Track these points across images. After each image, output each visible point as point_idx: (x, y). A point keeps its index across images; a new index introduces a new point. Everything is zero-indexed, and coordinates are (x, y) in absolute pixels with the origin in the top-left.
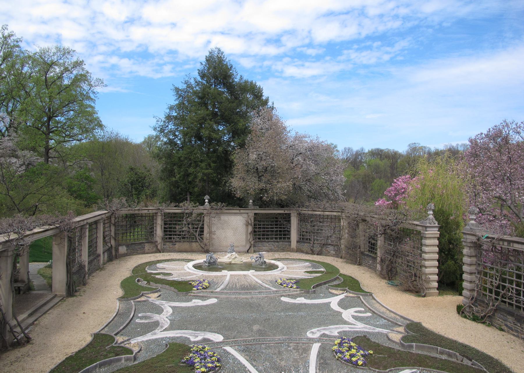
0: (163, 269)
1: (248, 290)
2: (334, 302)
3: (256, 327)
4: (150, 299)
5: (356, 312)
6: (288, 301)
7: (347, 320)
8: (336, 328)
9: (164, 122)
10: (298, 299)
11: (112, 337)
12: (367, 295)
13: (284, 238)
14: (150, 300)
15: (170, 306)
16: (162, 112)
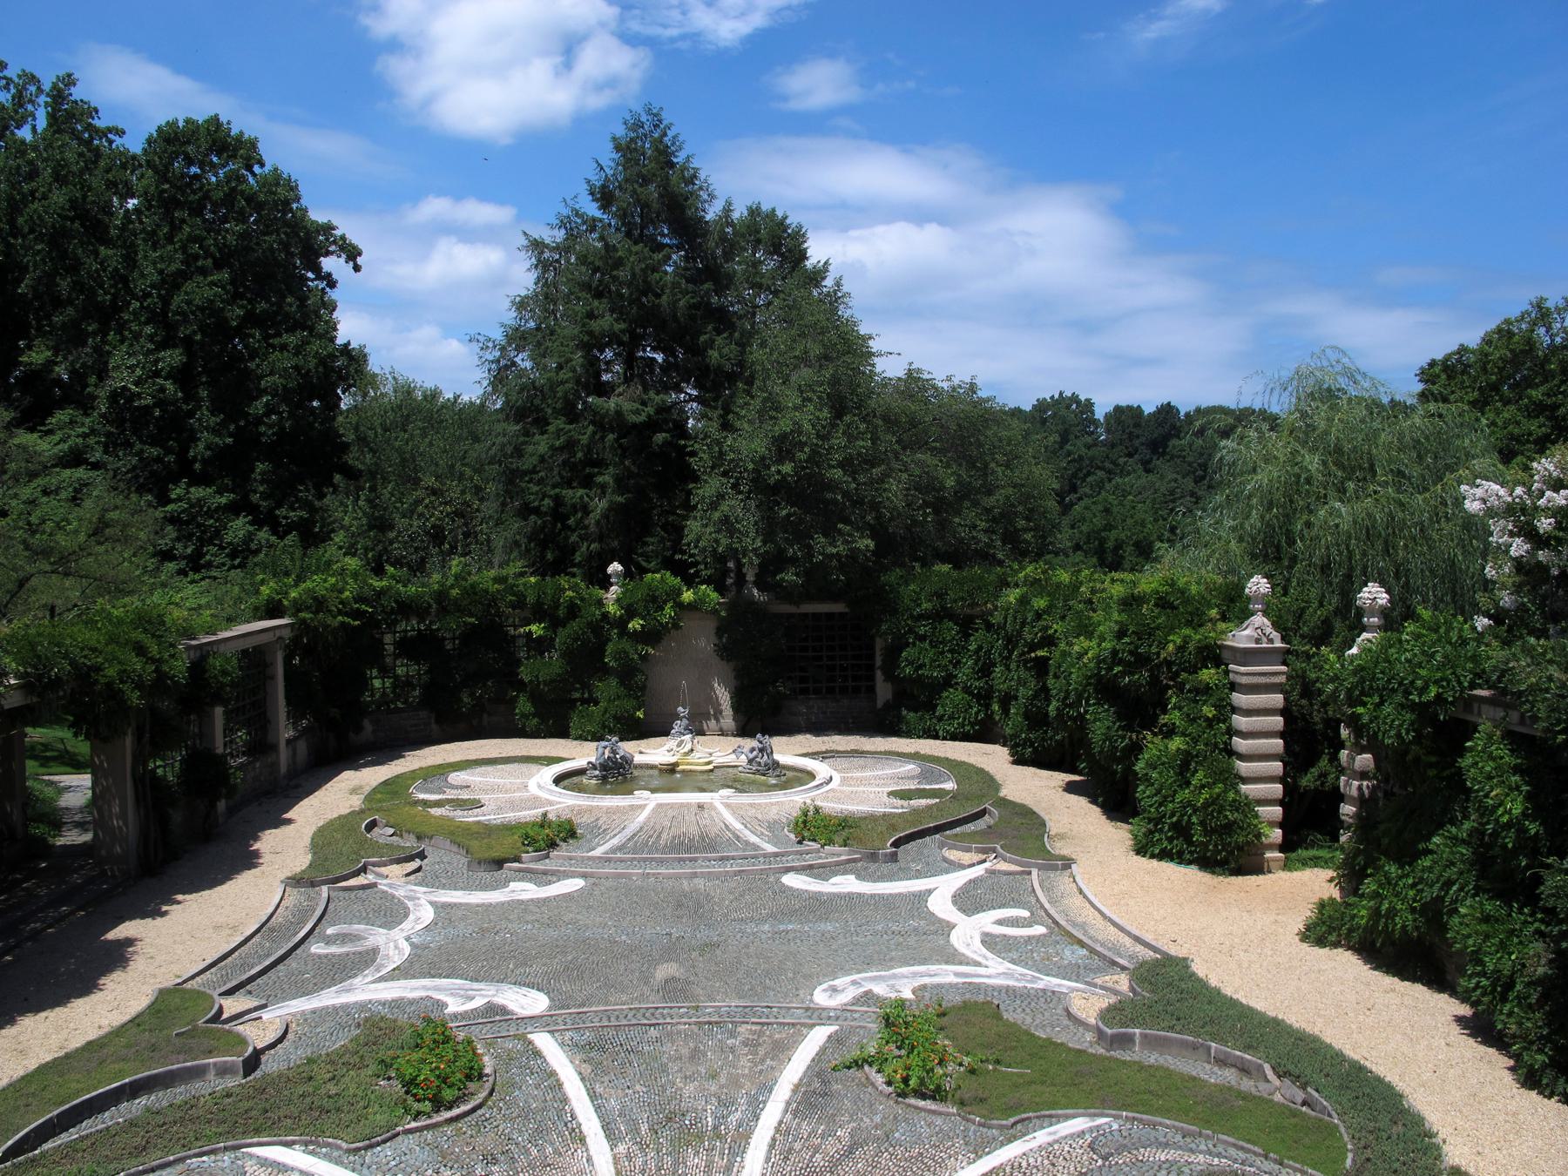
0: (462, 787)
1: (688, 851)
2: (941, 891)
3: (664, 971)
4: (385, 881)
5: (1000, 922)
6: (805, 887)
7: (962, 949)
8: (915, 975)
9: (503, 349)
10: (834, 880)
11: (211, 997)
12: (1054, 868)
14: (383, 885)
15: (431, 903)
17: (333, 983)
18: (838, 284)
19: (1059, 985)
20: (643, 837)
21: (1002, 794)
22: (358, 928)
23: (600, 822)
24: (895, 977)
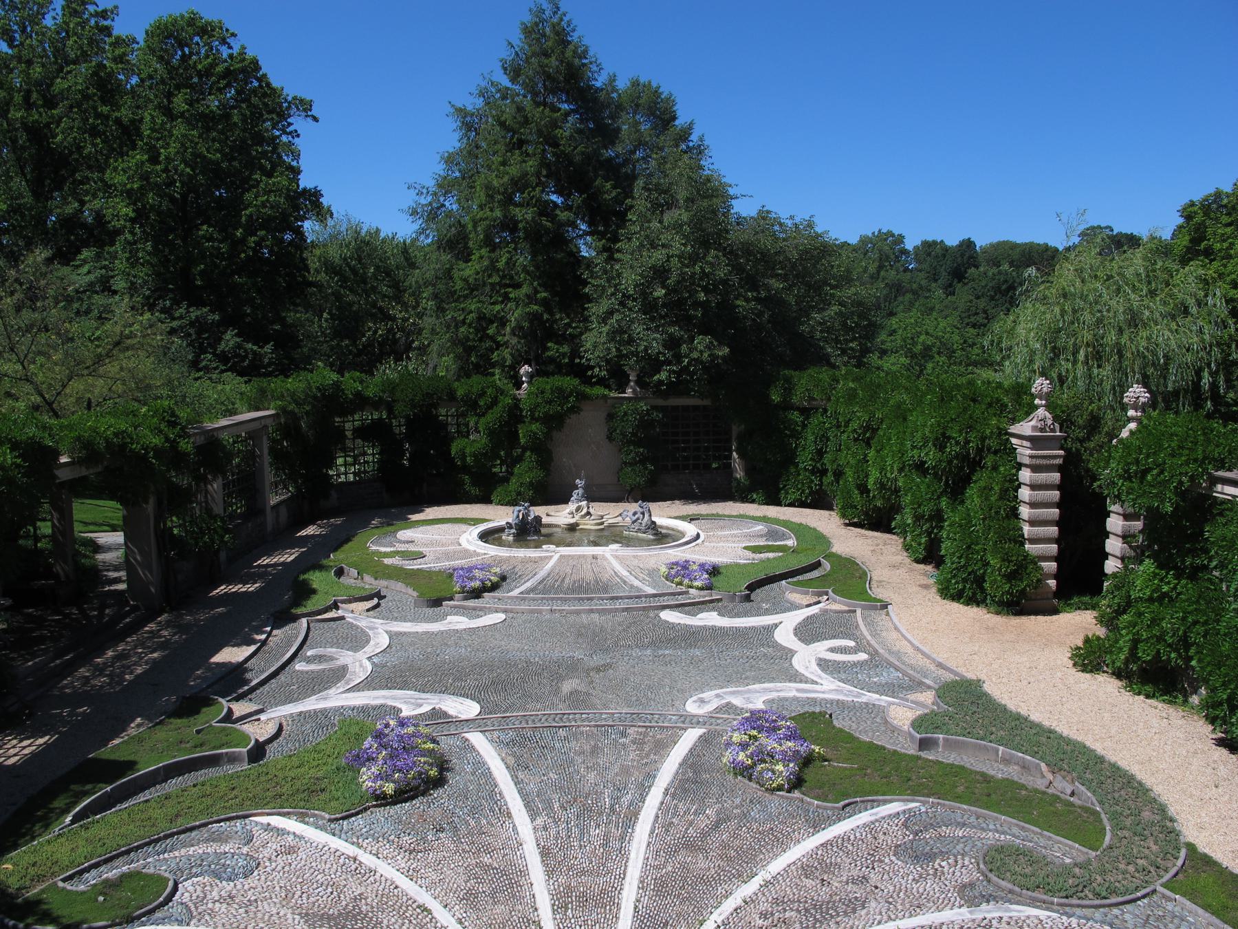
0: (408, 542)
2: (785, 625)
3: (567, 686)
5: (832, 650)
6: (676, 621)
7: (801, 670)
9: (435, 194)
12: (875, 608)
14: (350, 618)
15: (387, 632)
16: (430, 171)
17: (314, 693)
18: (701, 139)
21: (834, 550)
22: (331, 651)
23: (517, 570)
24: (749, 691)
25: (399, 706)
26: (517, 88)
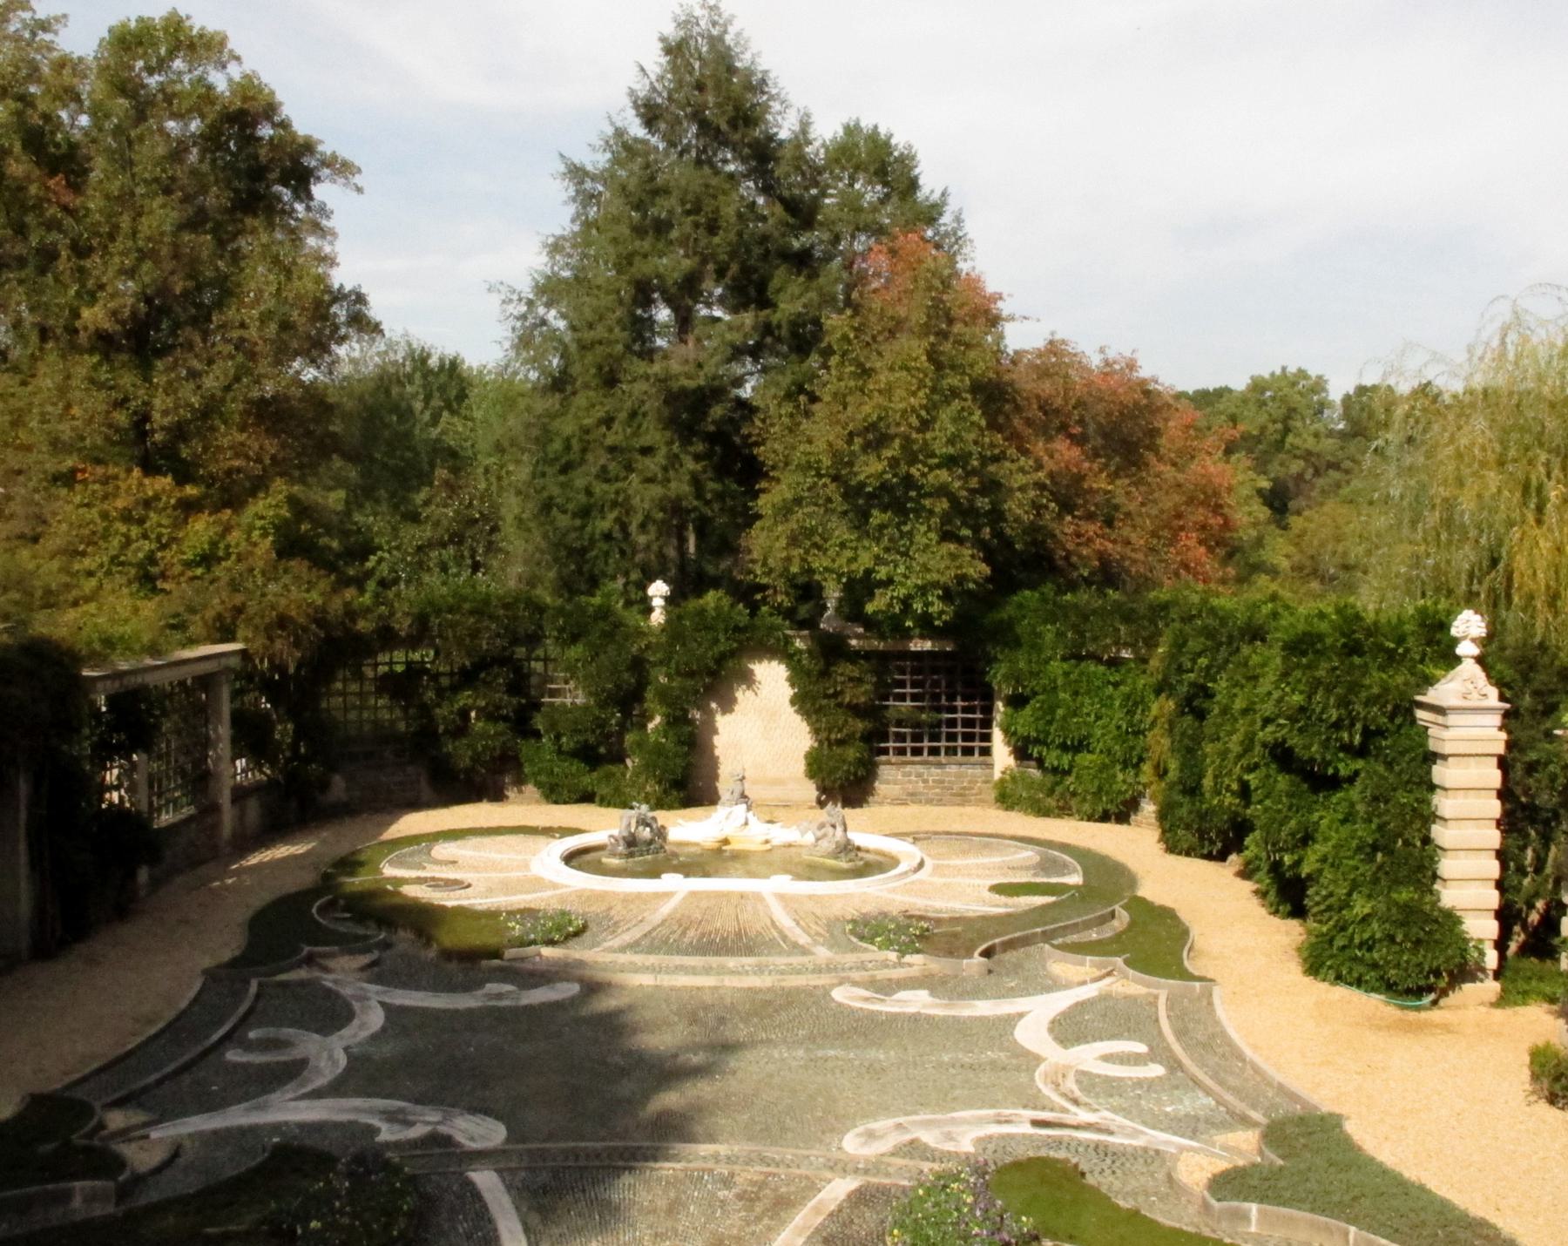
5: (1107, 1058)
8: (980, 1121)
9: (530, 303)
13: (968, 752)
14: (328, 981)
15: (382, 1004)
17: (246, 1098)
18: (958, 220)
19: (1167, 1143)
20: (664, 931)
21: (1140, 893)
22: (288, 1032)
23: (613, 913)
24: (953, 1121)
25: (375, 1122)
26: (654, 140)
